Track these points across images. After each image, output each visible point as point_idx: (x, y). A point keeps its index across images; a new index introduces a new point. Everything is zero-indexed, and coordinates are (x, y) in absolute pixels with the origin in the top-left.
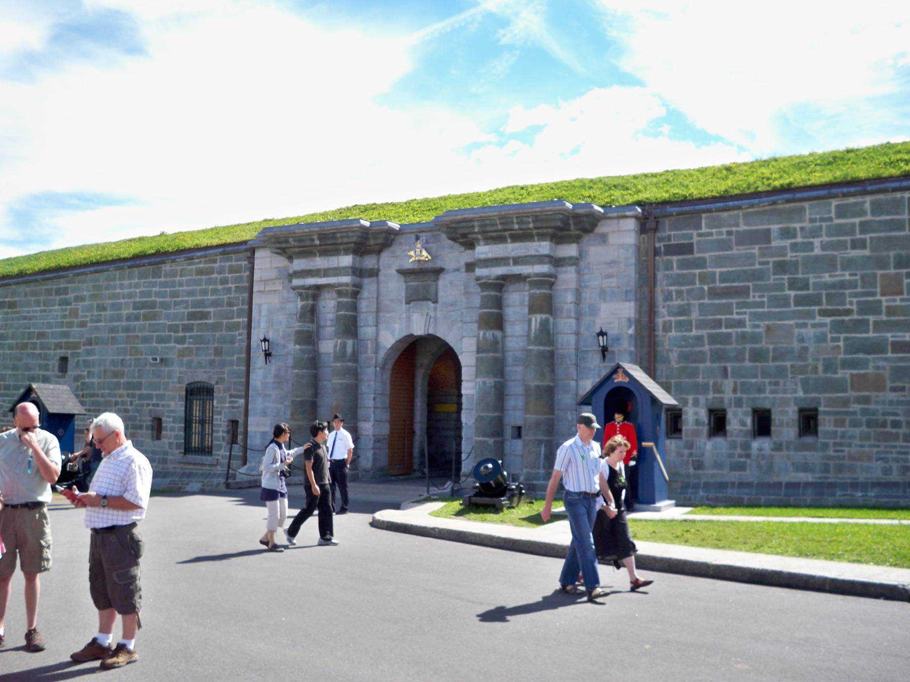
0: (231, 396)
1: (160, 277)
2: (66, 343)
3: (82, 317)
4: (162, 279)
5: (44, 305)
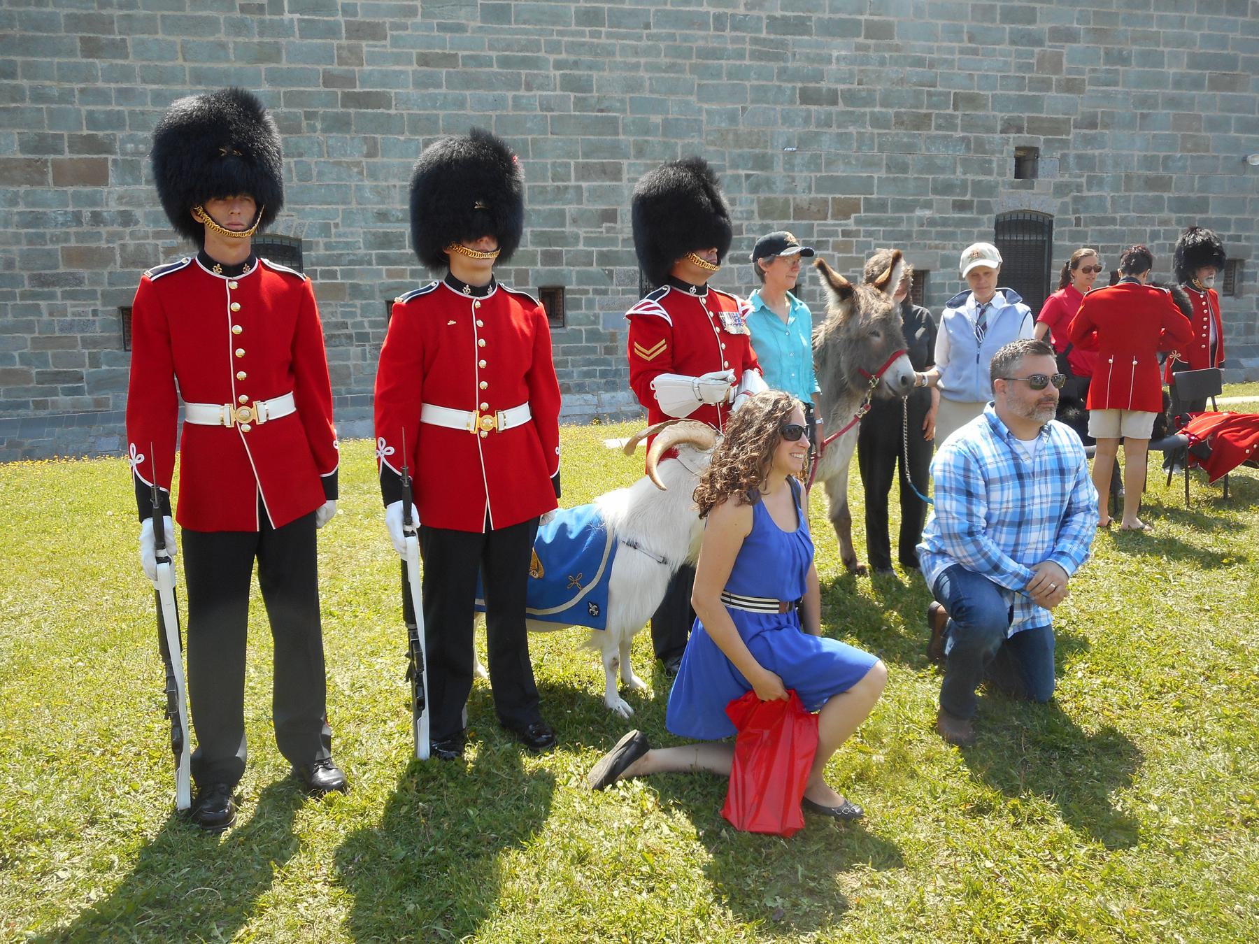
1: (1244, 14)
2: (1031, 120)
3: (1070, 71)
5: (971, 39)
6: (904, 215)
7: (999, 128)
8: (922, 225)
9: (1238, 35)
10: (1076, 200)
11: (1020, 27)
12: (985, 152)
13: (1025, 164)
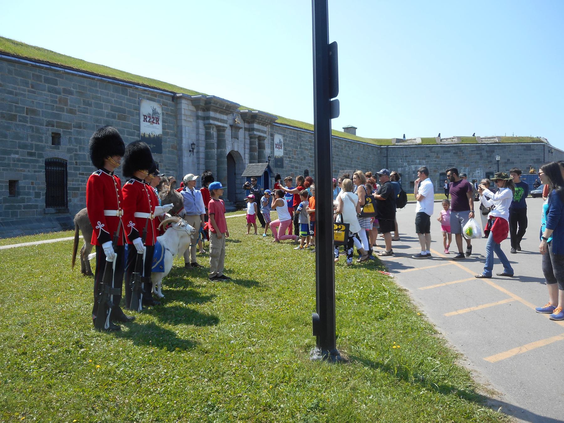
0: (167, 169)
2: (57, 122)
3: (71, 106)
4: (128, 97)
5: (32, 87)
6: (6, 156)
7: (45, 124)
8: (14, 161)
9: (126, 102)
10: (76, 155)
11: (52, 86)
12: (40, 133)
13: (56, 139)
